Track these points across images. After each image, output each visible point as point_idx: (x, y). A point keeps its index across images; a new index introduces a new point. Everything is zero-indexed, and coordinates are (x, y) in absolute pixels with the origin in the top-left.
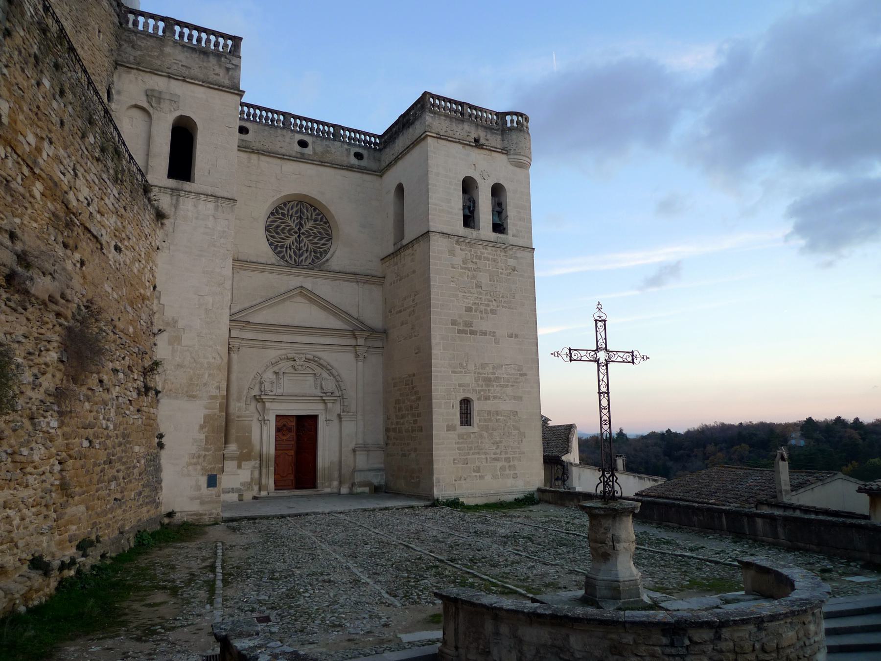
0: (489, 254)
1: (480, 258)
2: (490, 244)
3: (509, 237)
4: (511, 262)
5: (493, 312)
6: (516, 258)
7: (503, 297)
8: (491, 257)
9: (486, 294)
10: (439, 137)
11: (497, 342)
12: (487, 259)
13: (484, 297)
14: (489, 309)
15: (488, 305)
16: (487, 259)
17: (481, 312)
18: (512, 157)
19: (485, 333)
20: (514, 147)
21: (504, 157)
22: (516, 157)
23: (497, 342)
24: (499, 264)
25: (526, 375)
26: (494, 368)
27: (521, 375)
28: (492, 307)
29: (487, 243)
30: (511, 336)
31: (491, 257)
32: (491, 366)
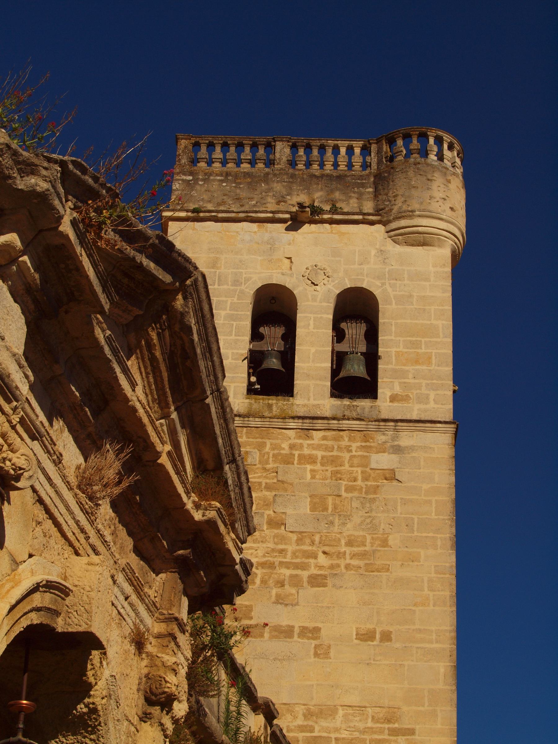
0: (318, 447)
1: (287, 460)
2: (319, 424)
3: (384, 404)
4: (383, 461)
5: (317, 581)
6: (398, 450)
7: (350, 543)
8: (319, 454)
9: (299, 541)
10: (197, 216)
11: (322, 652)
12: (312, 460)
13: (290, 548)
14: (305, 574)
15: (304, 567)
16: (312, 460)
17: (281, 584)
18: (394, 225)
19: (286, 632)
20: (399, 201)
21: (379, 228)
22: (403, 223)
23: (322, 652)
24: (347, 467)
25: (412, 732)
26: (308, 715)
27: (394, 732)
28: (314, 571)
29: (307, 424)
30: (367, 636)
31: (319, 454)
32: (300, 710)
